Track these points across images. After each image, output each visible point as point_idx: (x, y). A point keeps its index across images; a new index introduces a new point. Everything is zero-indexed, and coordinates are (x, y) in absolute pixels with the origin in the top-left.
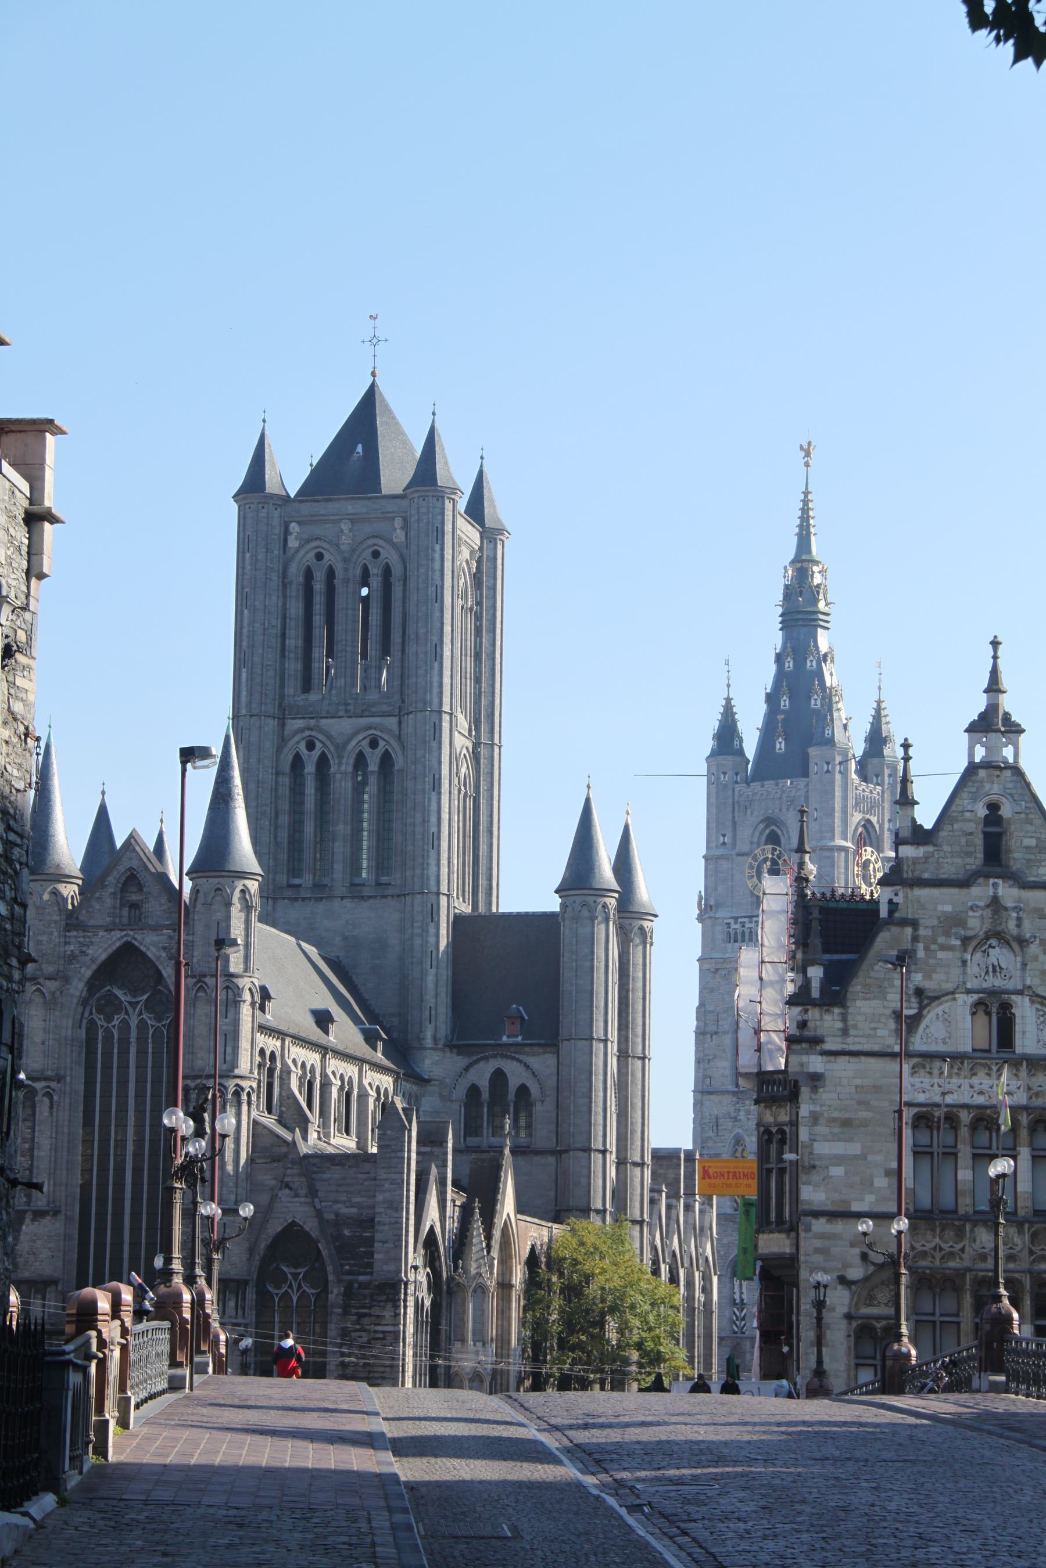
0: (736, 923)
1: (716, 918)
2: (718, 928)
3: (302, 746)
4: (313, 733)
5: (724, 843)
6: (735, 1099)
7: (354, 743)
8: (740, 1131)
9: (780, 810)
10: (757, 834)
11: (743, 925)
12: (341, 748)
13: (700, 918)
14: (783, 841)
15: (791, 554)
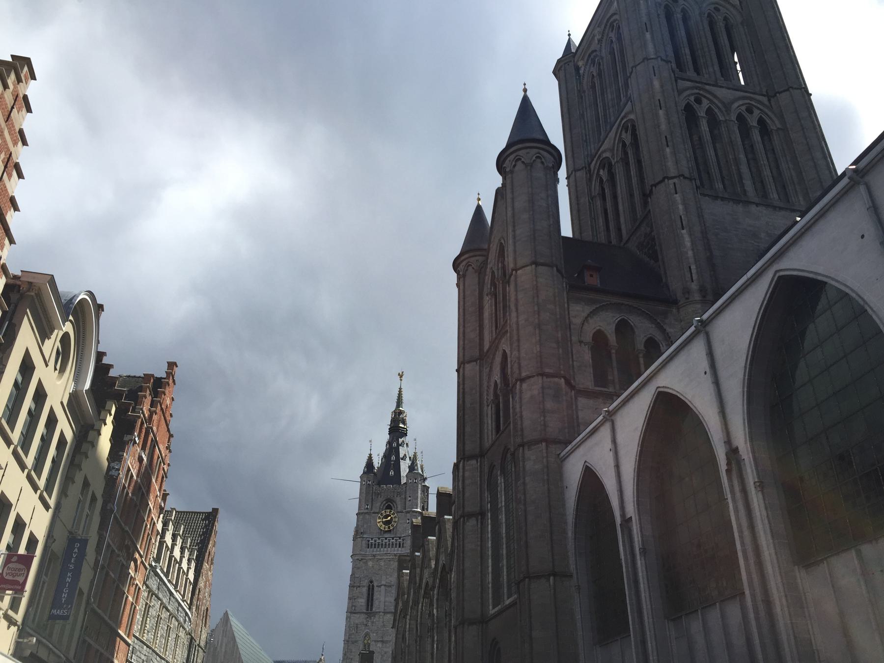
0: (372, 540)
1: (363, 538)
2: (364, 542)
3: (692, 98)
4: (701, 92)
5: (367, 508)
6: (366, 616)
7: (736, 105)
8: (368, 630)
9: (394, 496)
10: (382, 505)
11: (375, 541)
12: (727, 107)
13: (353, 540)
14: (393, 509)
15: (393, 407)
